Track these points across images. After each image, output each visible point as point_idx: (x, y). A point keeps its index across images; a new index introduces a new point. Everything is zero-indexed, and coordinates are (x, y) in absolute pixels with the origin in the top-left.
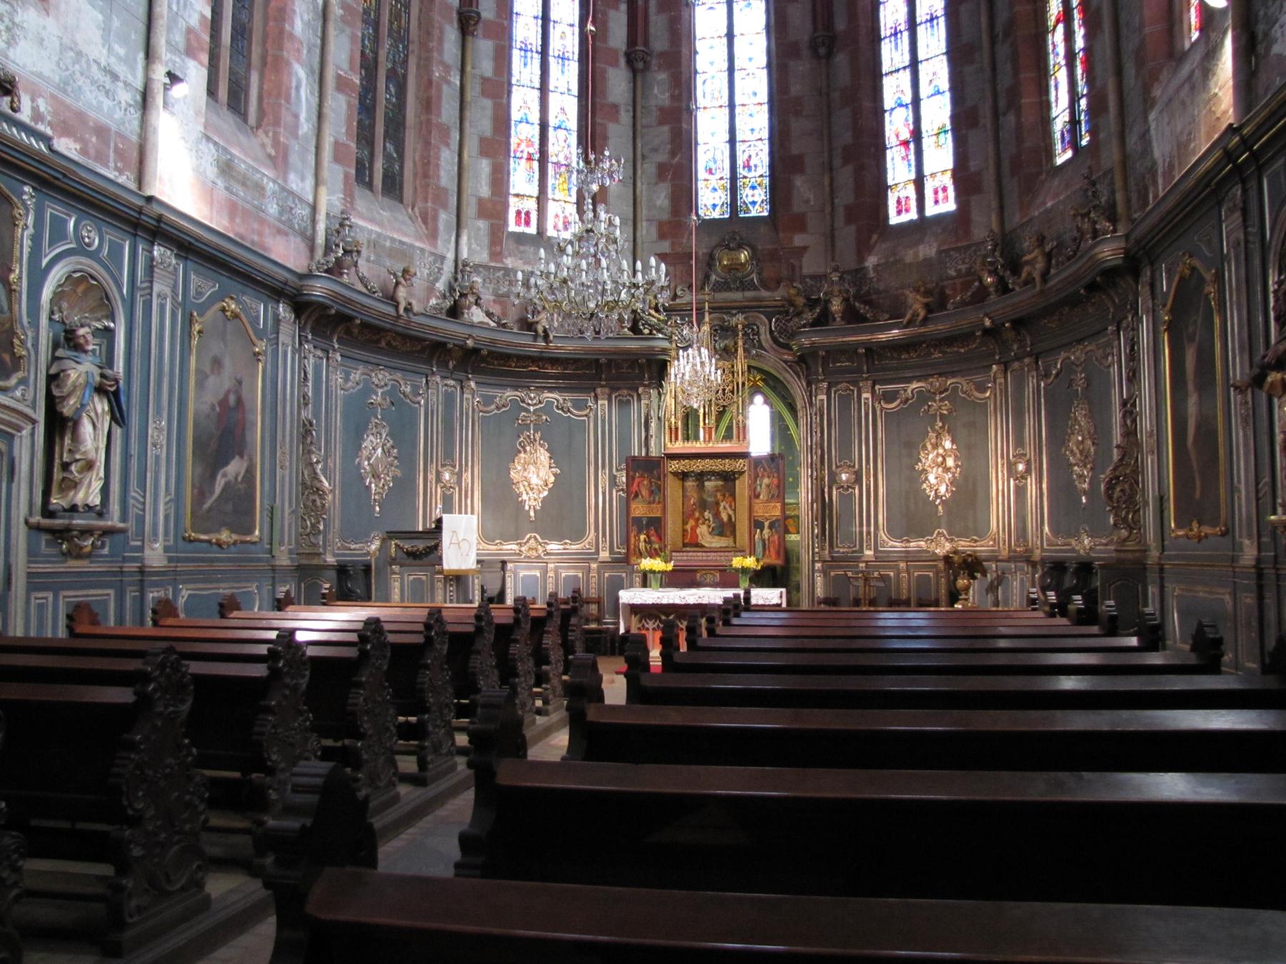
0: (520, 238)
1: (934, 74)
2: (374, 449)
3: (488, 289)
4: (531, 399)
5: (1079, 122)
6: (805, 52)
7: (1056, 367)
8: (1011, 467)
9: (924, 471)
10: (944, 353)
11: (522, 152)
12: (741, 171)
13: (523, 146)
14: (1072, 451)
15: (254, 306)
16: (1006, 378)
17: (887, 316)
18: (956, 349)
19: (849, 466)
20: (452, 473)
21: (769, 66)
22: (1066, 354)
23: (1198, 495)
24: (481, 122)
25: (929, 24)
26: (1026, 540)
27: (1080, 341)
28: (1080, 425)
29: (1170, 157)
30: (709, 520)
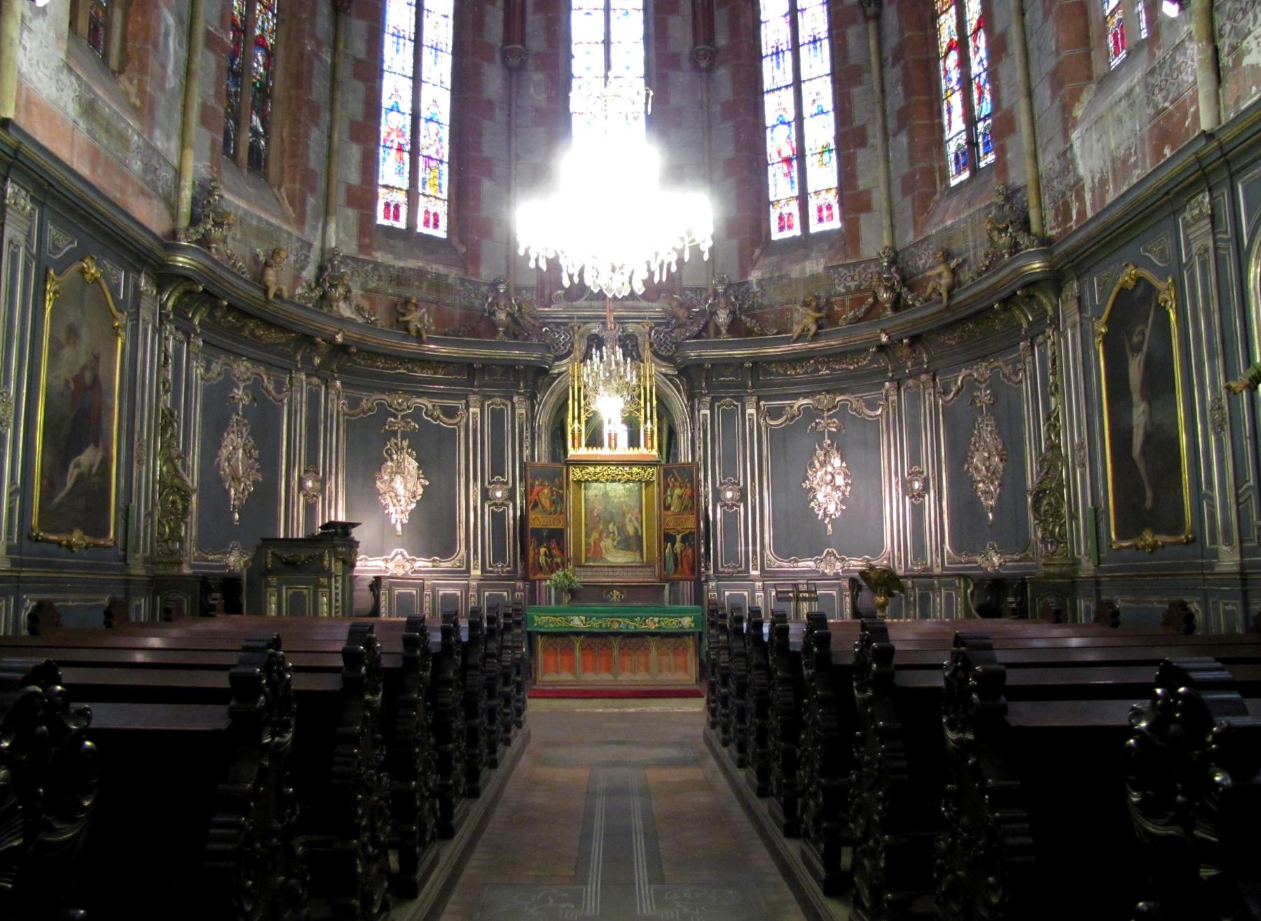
0: (390, 231)
1: (818, 94)
2: (234, 448)
3: (356, 282)
5: (977, 144)
6: (686, 64)
11: (392, 141)
13: (393, 136)
14: (976, 468)
15: (114, 272)
16: (899, 395)
17: (775, 331)
18: (845, 366)
19: (734, 483)
20: (316, 480)
22: (968, 371)
23: (1149, 503)
24: (352, 105)
25: (811, 46)
27: (984, 358)
30: (613, 533)
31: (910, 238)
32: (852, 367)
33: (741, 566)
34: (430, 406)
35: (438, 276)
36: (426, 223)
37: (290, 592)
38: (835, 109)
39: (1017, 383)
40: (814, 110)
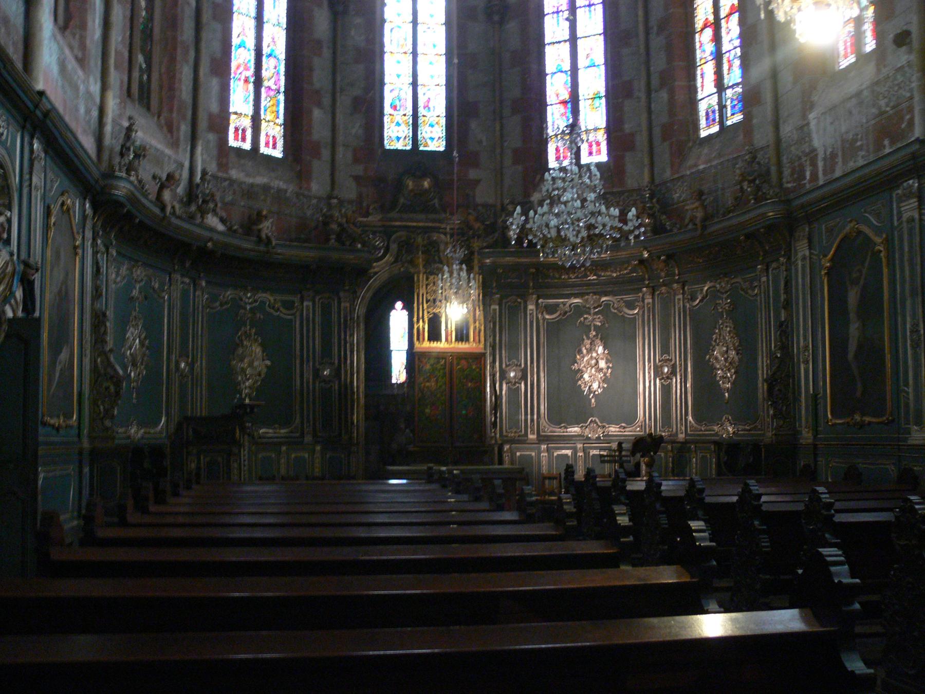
0: (239, 150)
4: (247, 298)
7: (701, 293)
8: (658, 372)
9: (580, 372)
10: (599, 276)
11: (240, 73)
12: (421, 111)
13: (241, 69)
14: (716, 358)
18: (608, 274)
19: (517, 365)
21: (448, 24)
22: (712, 284)
26: (670, 426)
27: (725, 275)
28: (724, 338)
29: (834, 148)
31: (668, 174)
32: (615, 275)
33: (521, 431)
34: (272, 301)
35: (279, 191)
36: (267, 144)
37: (208, 459)
38: (606, 64)
39: (753, 296)
40: (588, 63)
